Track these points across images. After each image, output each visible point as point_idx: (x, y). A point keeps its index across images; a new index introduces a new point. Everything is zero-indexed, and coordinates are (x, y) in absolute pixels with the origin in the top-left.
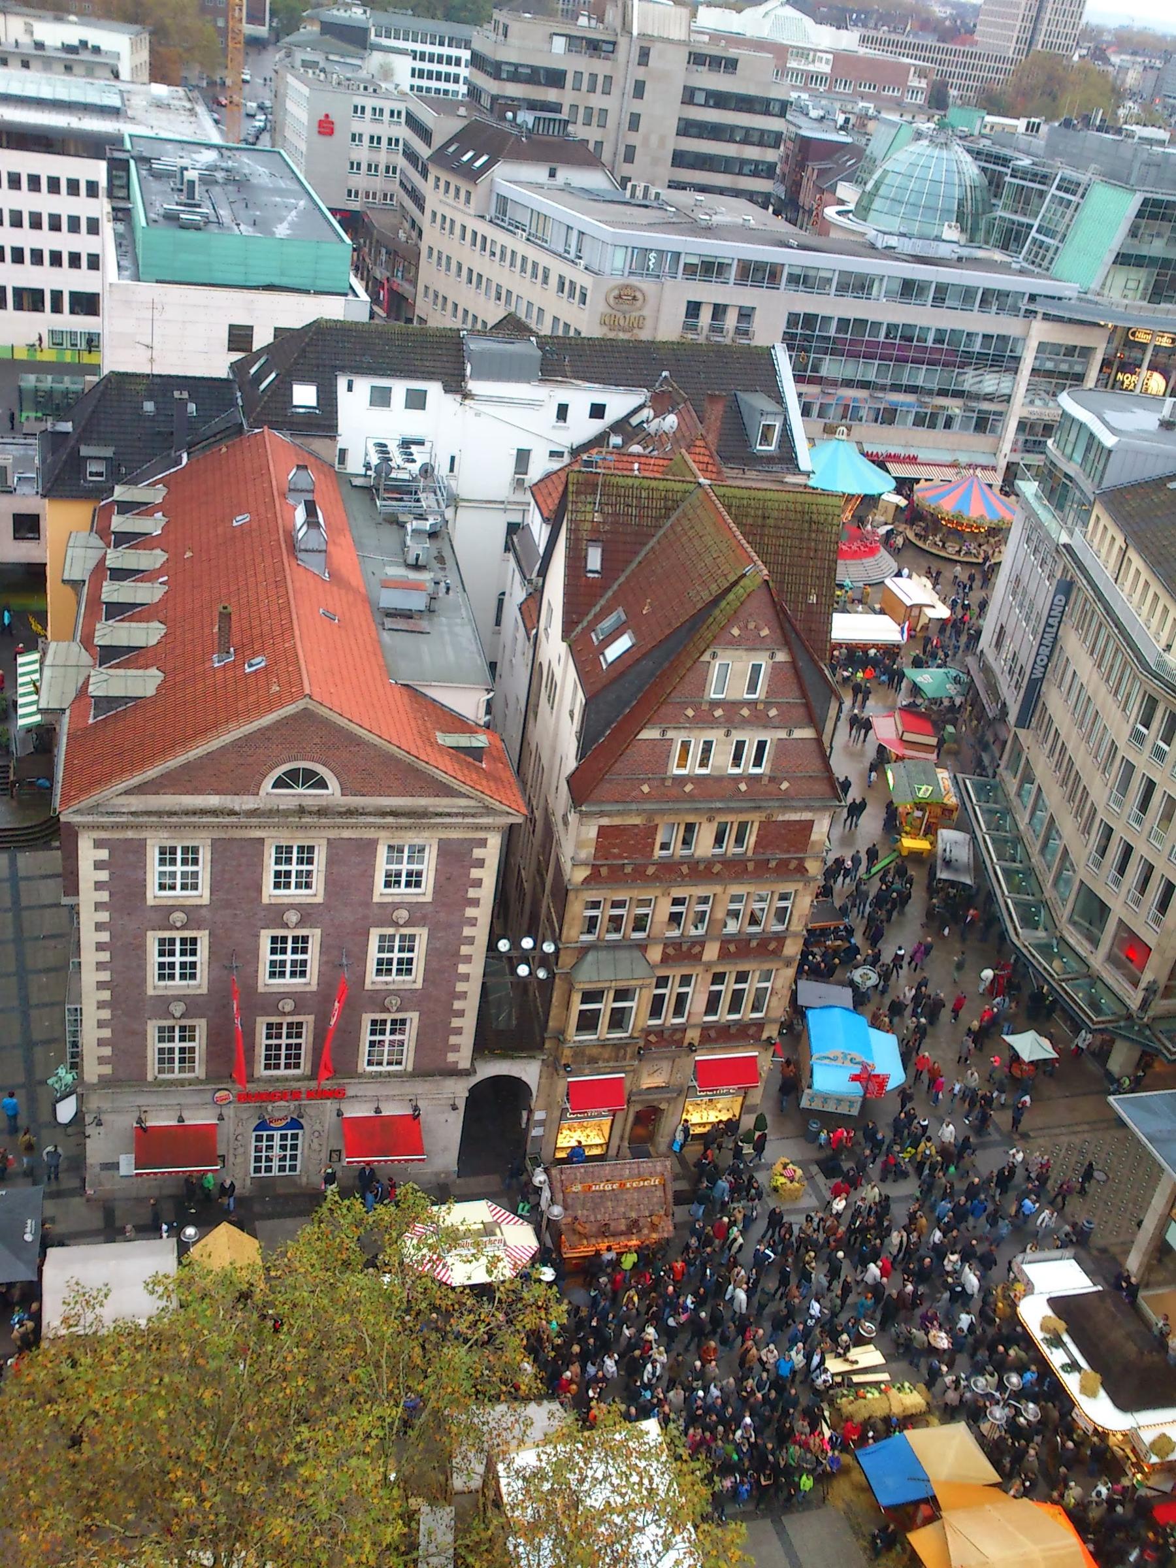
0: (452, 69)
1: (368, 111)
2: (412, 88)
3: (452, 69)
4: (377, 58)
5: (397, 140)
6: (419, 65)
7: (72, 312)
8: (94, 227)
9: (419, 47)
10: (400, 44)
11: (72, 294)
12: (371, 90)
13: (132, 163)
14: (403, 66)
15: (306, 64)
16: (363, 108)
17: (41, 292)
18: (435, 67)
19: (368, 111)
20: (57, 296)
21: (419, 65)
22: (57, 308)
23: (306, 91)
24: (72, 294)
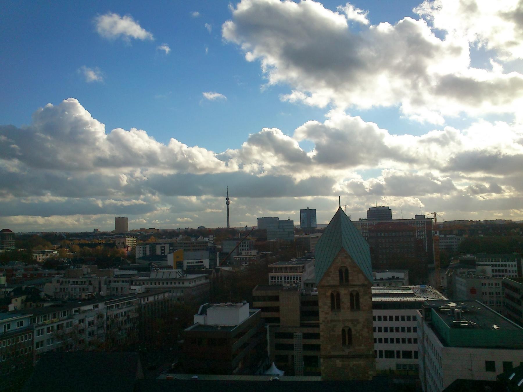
0: (503, 268)
1: (487, 285)
2: (493, 276)
3: (503, 268)
4: (479, 268)
5: (499, 293)
6: (494, 268)
7: (403, 358)
8: (415, 330)
9: (494, 263)
10: (488, 263)
11: (403, 351)
12: (487, 278)
13: (432, 309)
14: (489, 269)
15: (460, 273)
16: (485, 284)
17: (393, 352)
18: (501, 268)
19: (487, 285)
20: (398, 352)
21: (494, 268)
22: (398, 357)
23: (464, 281)
24: (403, 351)
